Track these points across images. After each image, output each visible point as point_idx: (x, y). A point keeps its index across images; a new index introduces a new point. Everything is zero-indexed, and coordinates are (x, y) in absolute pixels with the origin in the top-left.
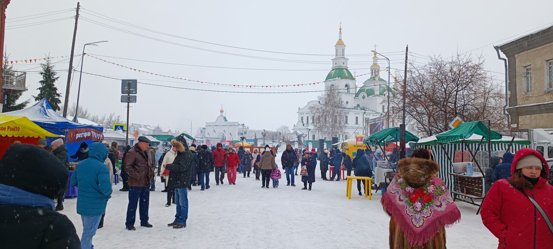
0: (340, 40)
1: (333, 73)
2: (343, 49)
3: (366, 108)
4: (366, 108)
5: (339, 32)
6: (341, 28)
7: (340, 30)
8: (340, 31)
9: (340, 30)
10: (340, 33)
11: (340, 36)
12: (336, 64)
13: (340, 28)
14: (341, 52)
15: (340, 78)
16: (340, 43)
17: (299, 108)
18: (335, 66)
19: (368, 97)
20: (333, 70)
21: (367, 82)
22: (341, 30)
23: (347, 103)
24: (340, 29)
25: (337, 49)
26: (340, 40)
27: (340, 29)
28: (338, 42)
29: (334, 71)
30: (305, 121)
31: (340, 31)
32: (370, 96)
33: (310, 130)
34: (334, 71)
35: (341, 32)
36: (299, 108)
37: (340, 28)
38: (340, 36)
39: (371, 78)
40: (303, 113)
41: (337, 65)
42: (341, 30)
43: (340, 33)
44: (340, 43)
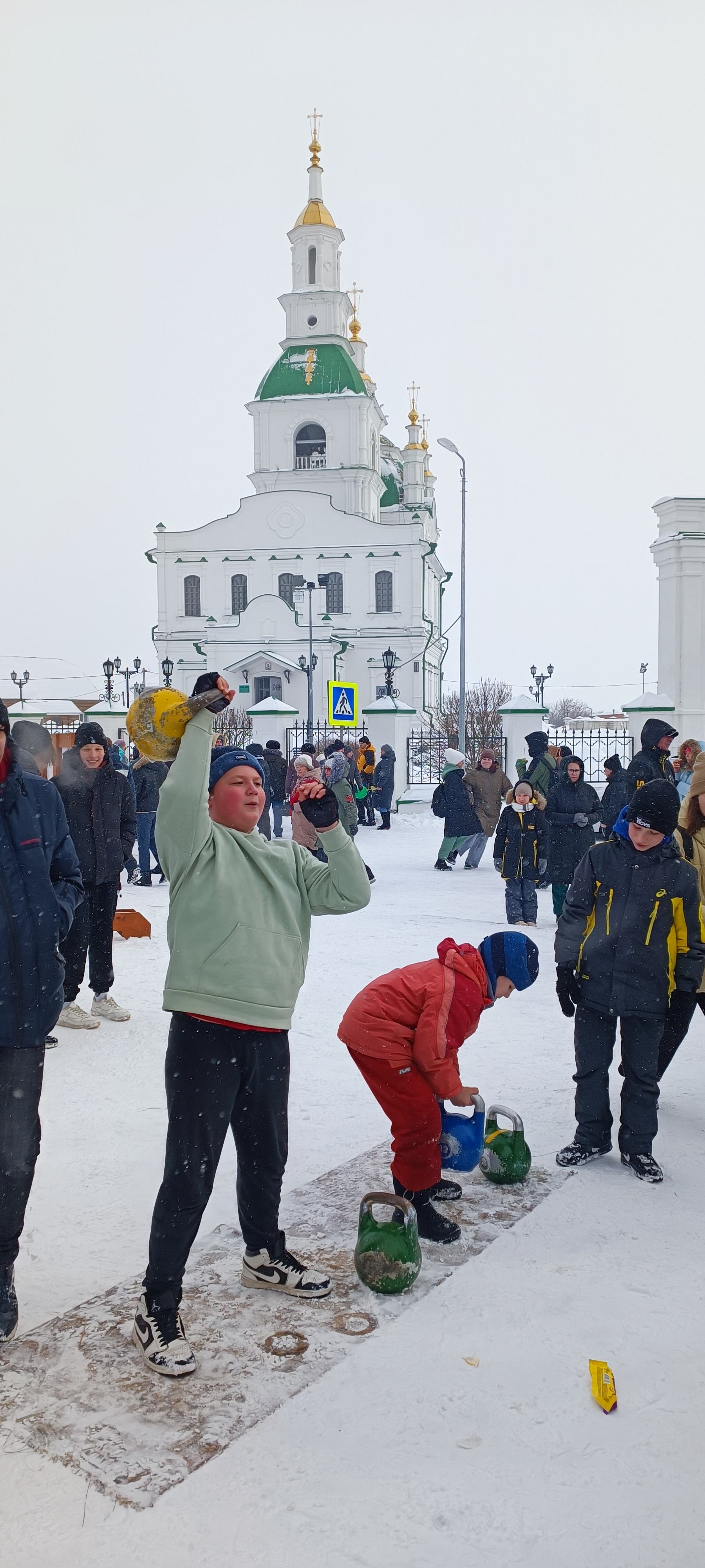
0: (315, 202)
1: (310, 367)
5: (310, 164)
6: (320, 143)
7: (311, 155)
8: (315, 158)
11: (314, 184)
12: (312, 321)
13: (315, 142)
15: (362, 394)
17: (161, 525)
18: (307, 331)
20: (291, 350)
24: (314, 148)
25: (313, 252)
26: (315, 202)
27: (314, 148)
28: (307, 212)
31: (315, 158)
35: (320, 164)
36: (161, 525)
37: (315, 142)
38: (314, 184)
40: (296, 553)
41: (317, 330)
42: (318, 155)
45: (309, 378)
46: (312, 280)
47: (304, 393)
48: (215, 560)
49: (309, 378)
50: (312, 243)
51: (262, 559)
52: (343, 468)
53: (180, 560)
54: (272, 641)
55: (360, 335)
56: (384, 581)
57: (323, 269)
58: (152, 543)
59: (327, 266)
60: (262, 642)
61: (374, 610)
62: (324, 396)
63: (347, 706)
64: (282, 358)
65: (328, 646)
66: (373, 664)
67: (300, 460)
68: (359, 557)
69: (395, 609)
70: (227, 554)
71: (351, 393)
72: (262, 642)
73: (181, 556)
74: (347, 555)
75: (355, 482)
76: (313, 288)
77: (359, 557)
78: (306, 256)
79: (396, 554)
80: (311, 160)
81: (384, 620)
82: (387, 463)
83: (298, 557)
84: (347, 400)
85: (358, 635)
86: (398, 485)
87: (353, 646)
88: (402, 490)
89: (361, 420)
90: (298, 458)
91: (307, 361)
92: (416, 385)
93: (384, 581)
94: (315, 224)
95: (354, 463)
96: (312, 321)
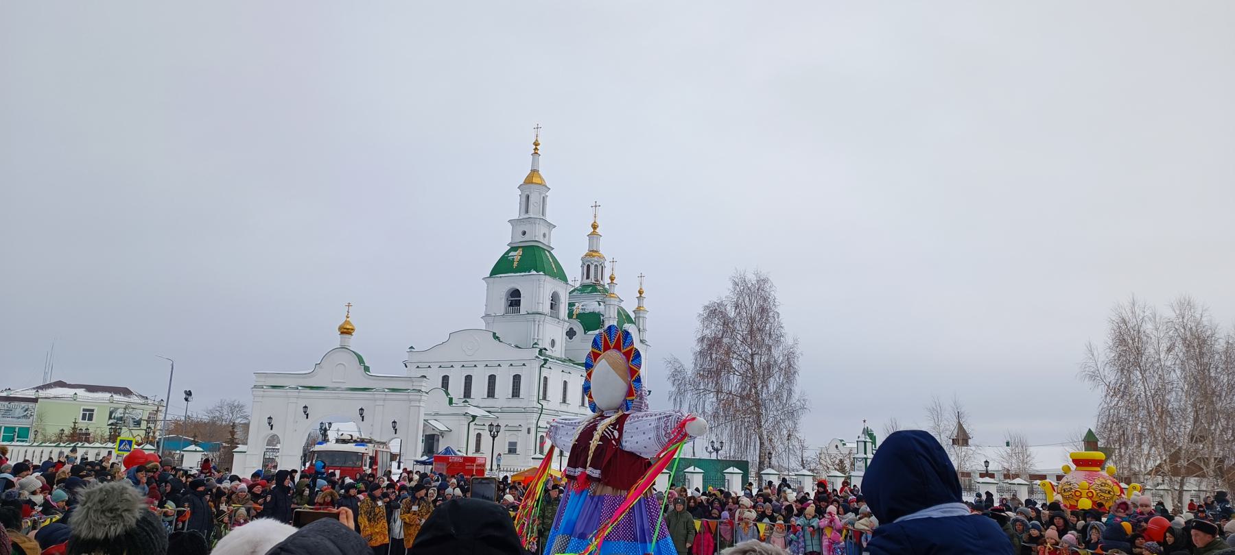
0: (534, 172)
1: (517, 258)
2: (544, 197)
5: (533, 152)
7: (534, 147)
8: (536, 149)
9: (534, 147)
10: (536, 153)
12: (524, 233)
13: (537, 140)
14: (540, 205)
15: (541, 273)
16: (532, 180)
17: (412, 347)
18: (519, 238)
19: (585, 333)
20: (514, 249)
21: (574, 293)
22: (538, 147)
23: (553, 343)
24: (536, 144)
25: (528, 197)
26: (534, 172)
27: (536, 144)
29: (520, 252)
30: (457, 388)
31: (536, 149)
32: (590, 333)
33: (474, 417)
34: (520, 252)
35: (539, 152)
36: (412, 347)
37: (537, 140)
38: (535, 162)
39: (584, 287)
41: (526, 238)
42: (538, 147)
43: (536, 153)
44: (532, 180)
45: (515, 264)
46: (527, 212)
47: (511, 272)
48: (435, 367)
49: (515, 264)
50: (528, 193)
51: (457, 367)
52: (528, 314)
53: (418, 367)
54: (437, 414)
55: (597, 230)
56: (517, 379)
57: (532, 205)
58: (406, 357)
59: (535, 204)
60: (430, 414)
61: (486, 396)
62: (518, 274)
63: (128, 447)
64: (508, 252)
65: (463, 417)
66: (507, 428)
68: (505, 366)
69: (495, 397)
70: (441, 364)
71: (535, 273)
72: (430, 414)
73: (418, 364)
74: (499, 365)
75: (534, 321)
76: (527, 216)
77: (505, 366)
78: (524, 199)
79: (524, 365)
81: (515, 403)
82: (600, 305)
83: (475, 366)
84: (532, 276)
85: (500, 411)
86: (602, 318)
87: (498, 418)
88: (603, 321)
89: (539, 287)
91: (516, 255)
92: (615, 260)
93: (517, 379)
94: (529, 183)
95: (534, 311)
96: (524, 233)
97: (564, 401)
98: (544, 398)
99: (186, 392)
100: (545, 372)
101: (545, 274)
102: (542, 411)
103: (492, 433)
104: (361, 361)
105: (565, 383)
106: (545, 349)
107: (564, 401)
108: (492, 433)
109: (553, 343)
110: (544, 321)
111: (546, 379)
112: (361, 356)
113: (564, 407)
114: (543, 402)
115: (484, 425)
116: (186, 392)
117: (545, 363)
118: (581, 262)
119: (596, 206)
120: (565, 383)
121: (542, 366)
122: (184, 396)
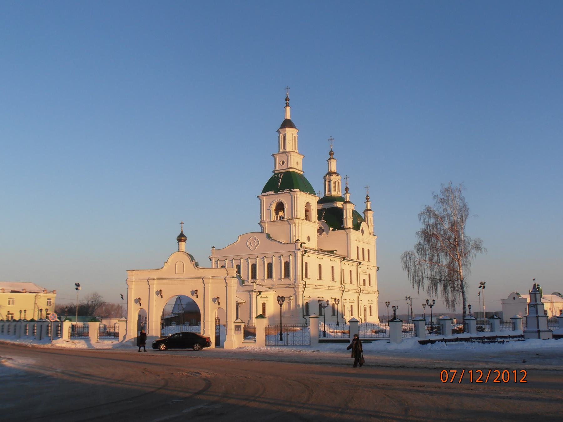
3: (336, 251)
4: (336, 251)
13: (287, 98)
22: (289, 102)
23: (309, 238)
36: (214, 247)
42: (289, 102)
67: (276, 216)
80: (286, 104)
90: (277, 216)
97: (320, 278)
98: (306, 277)
99: (76, 284)
100: (305, 259)
101: (300, 191)
102: (305, 286)
103: (280, 302)
104: (192, 258)
105: (320, 265)
106: (304, 243)
107: (320, 278)
108: (280, 302)
109: (309, 238)
110: (302, 224)
111: (306, 263)
112: (192, 256)
113: (320, 282)
114: (305, 280)
115: (267, 297)
116: (76, 284)
117: (305, 253)
118: (324, 179)
119: (331, 139)
120: (320, 265)
121: (303, 255)
122: (75, 287)
